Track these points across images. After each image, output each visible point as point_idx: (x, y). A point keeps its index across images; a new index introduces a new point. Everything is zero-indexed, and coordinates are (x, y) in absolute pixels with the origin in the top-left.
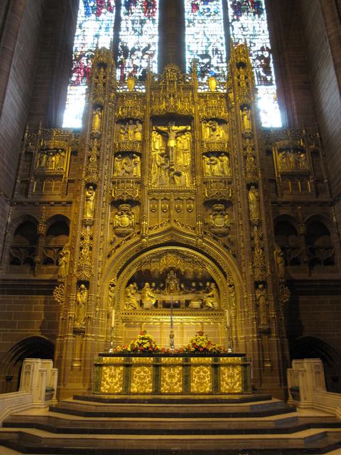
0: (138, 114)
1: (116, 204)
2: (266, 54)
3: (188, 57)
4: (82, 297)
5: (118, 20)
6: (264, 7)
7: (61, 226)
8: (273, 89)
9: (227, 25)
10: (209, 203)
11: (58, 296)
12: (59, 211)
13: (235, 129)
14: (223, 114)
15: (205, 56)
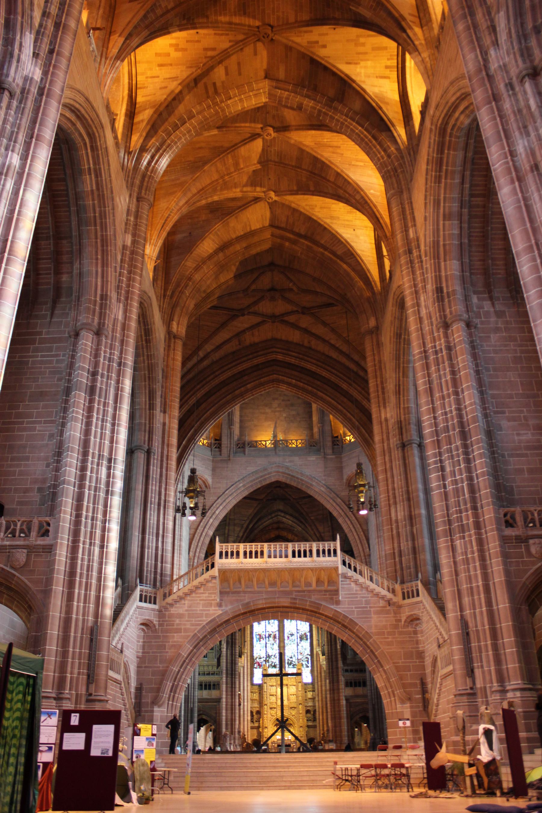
0: (275, 684)
1: (271, 708)
2: (309, 657)
3: (286, 658)
4: (266, 730)
5: (266, 643)
6: (309, 637)
7: (258, 713)
8: (310, 668)
9: (298, 645)
10: (291, 708)
11: (261, 730)
12: (258, 709)
13: (297, 688)
14: (295, 684)
15: (291, 658)
